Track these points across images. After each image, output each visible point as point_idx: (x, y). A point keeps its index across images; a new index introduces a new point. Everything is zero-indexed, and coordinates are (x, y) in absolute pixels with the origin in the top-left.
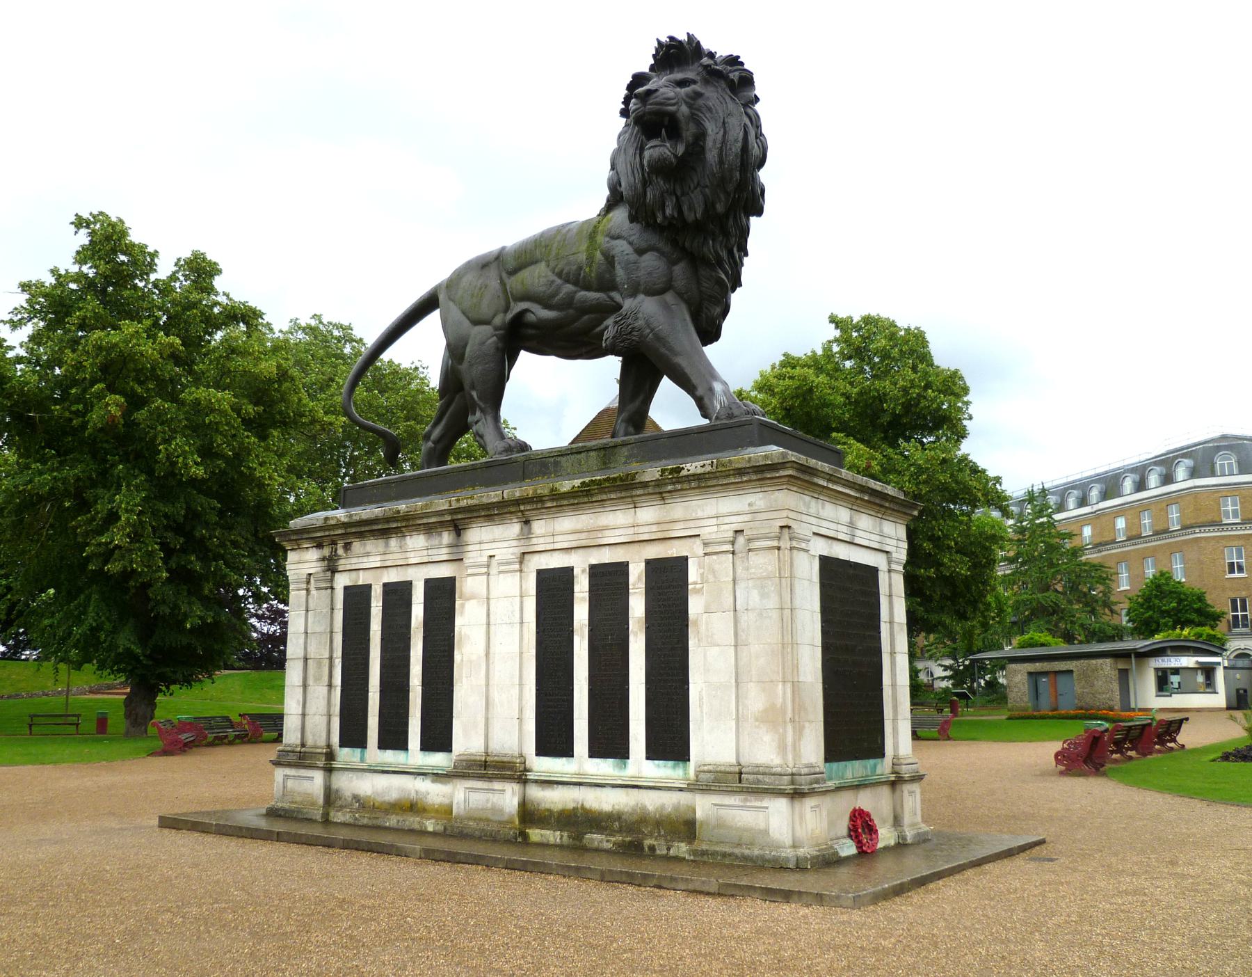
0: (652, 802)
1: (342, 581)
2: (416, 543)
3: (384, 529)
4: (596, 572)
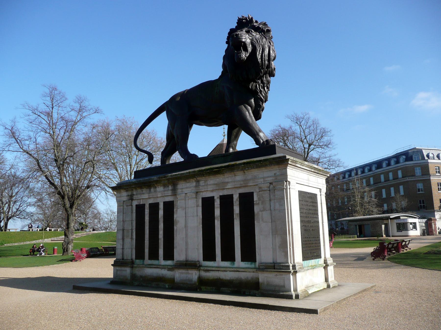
0: (243, 276)
1: (135, 203)
4: (222, 198)
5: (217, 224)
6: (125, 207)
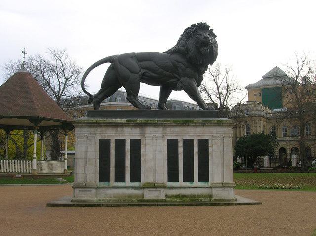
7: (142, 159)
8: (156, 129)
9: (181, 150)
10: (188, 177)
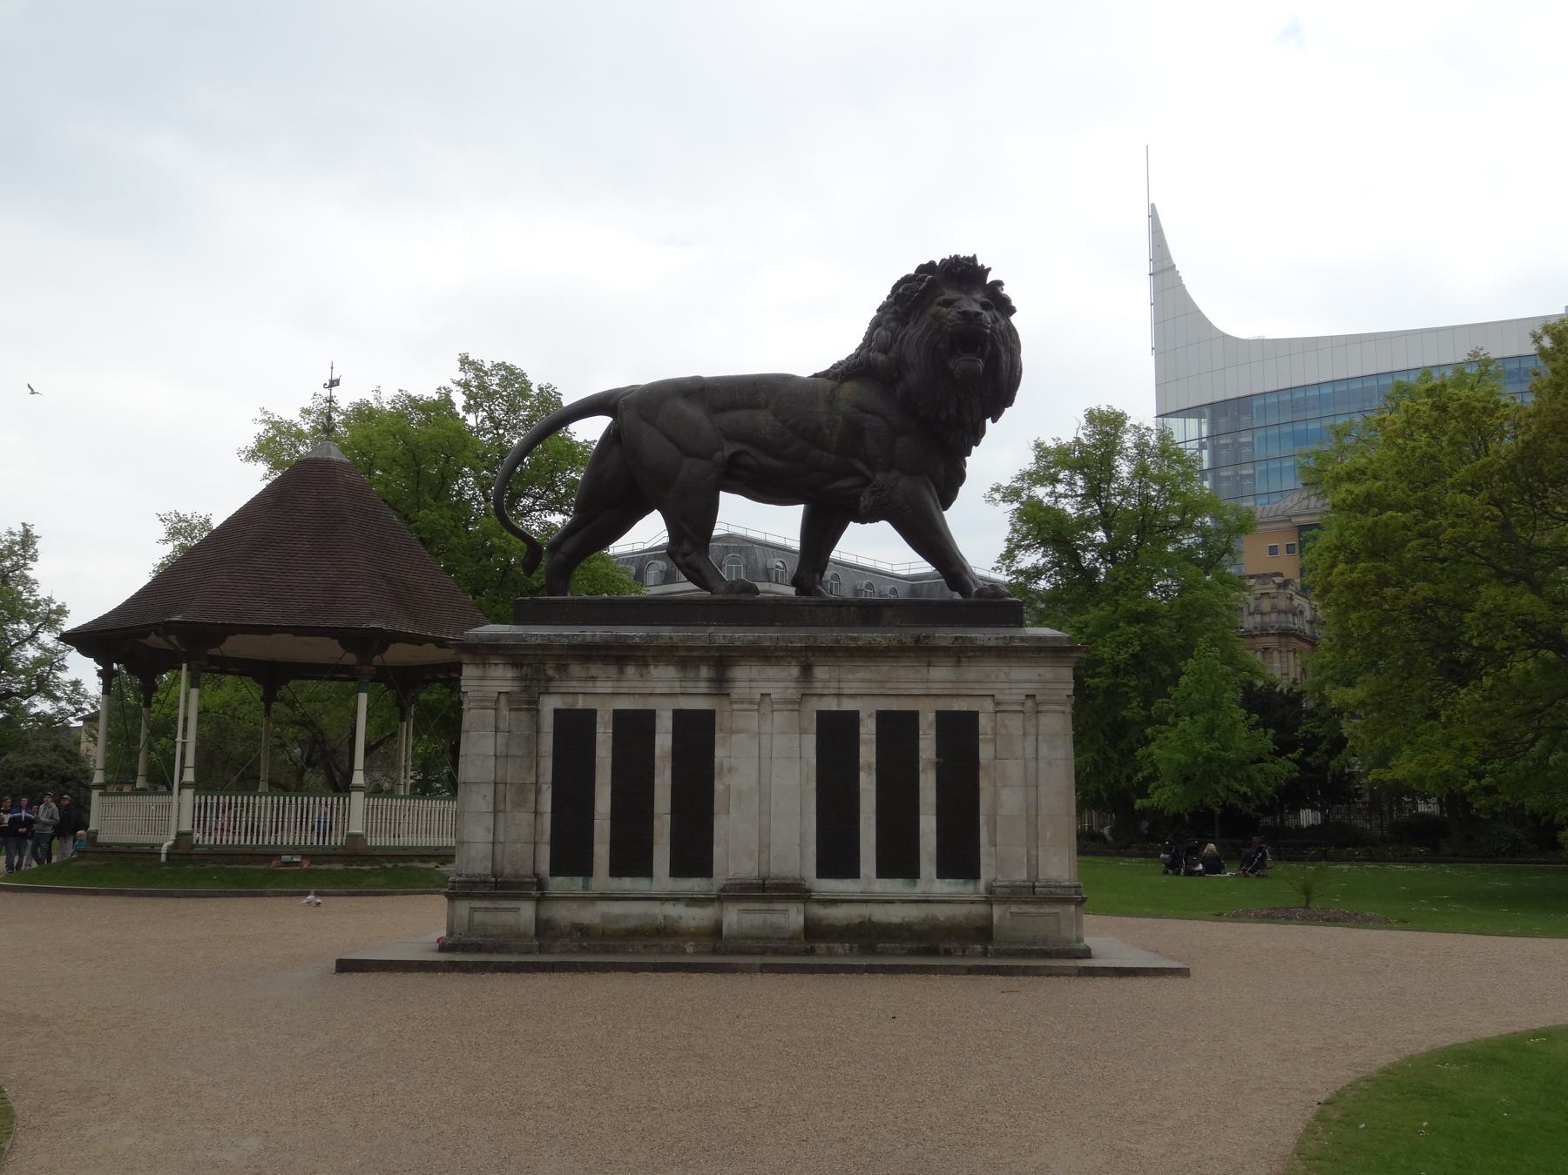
1: (550, 705)
2: (663, 676)
3: (619, 656)
5: (868, 784)
6: (504, 711)
7: (719, 786)
8: (772, 671)
9: (868, 753)
10: (898, 859)
